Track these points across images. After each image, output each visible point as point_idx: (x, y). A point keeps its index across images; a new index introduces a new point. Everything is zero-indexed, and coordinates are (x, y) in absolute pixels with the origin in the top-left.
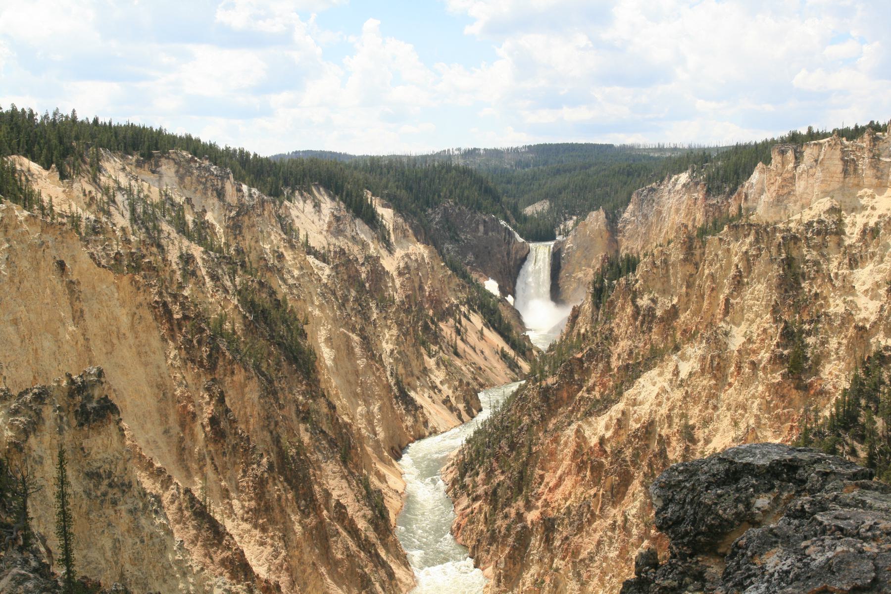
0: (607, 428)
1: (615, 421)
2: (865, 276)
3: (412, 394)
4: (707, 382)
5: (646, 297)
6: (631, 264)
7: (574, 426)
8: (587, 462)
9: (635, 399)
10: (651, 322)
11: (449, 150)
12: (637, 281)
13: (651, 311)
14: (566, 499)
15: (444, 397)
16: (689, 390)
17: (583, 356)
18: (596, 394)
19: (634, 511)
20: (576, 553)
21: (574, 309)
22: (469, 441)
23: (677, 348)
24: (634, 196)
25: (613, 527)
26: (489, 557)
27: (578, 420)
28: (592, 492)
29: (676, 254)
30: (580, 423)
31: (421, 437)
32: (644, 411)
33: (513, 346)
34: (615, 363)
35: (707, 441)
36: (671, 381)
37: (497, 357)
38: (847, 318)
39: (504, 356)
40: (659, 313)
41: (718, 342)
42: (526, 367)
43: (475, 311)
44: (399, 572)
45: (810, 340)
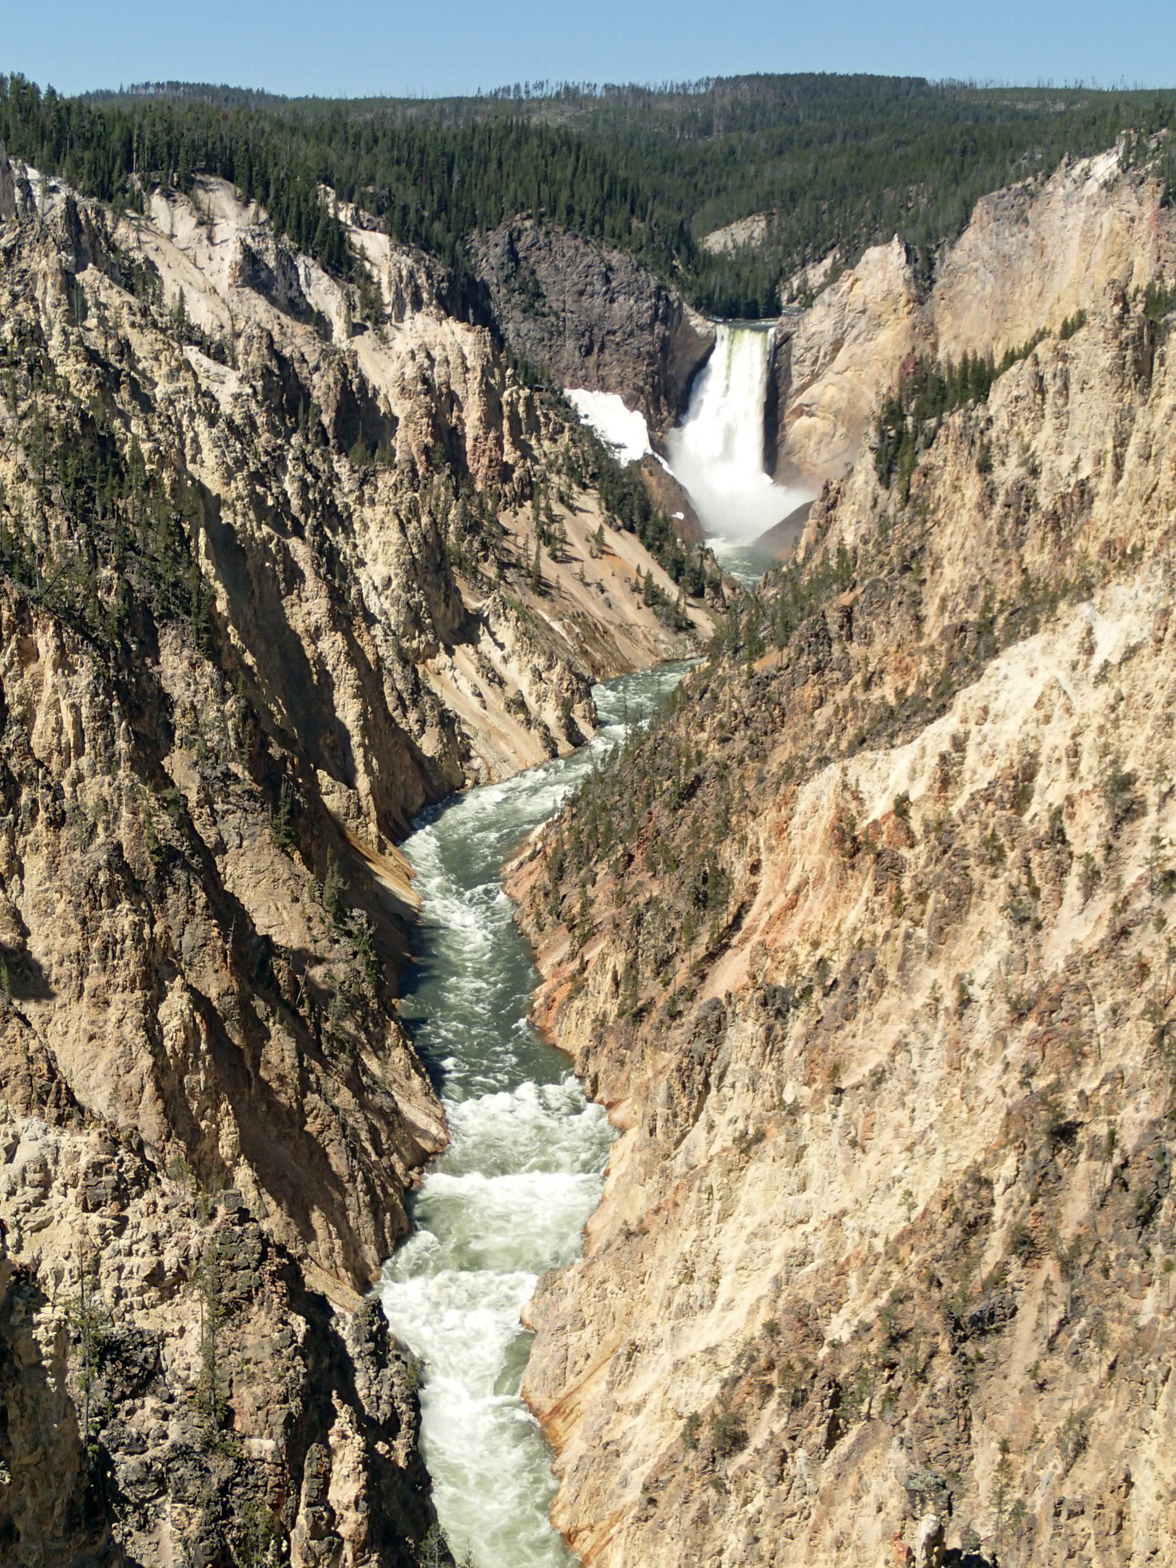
0: (913, 775)
1: (932, 761)
3: (434, 685)
5: (1013, 461)
6: (978, 379)
7: (833, 771)
9: (985, 710)
10: (1020, 521)
11: (517, 87)
12: (990, 421)
13: (1022, 500)
14: (816, 945)
15: (510, 693)
16: (1125, 692)
17: (856, 599)
18: (886, 692)
19: (981, 976)
21: (826, 488)
22: (573, 802)
24: (978, 211)
26: (623, 1078)
27: (842, 756)
28: (881, 930)
29: (1094, 353)
30: (846, 762)
32: (1007, 734)
33: (677, 570)
36: (1074, 668)
37: (639, 598)
39: (653, 598)
40: (1045, 501)
43: (585, 487)
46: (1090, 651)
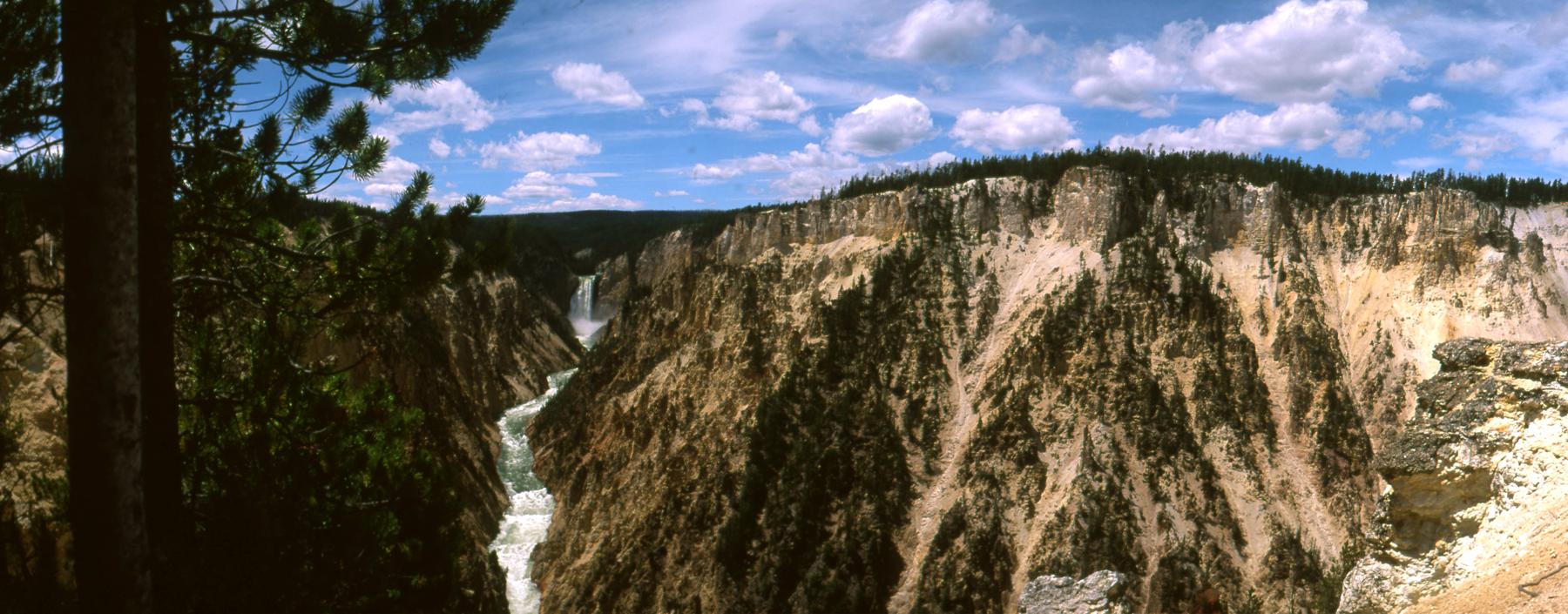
2: (797, 299)
4: (700, 368)
6: (647, 291)
8: (622, 422)
20: (617, 484)
23: (678, 347)
25: (642, 466)
29: (678, 284)
31: (511, 406)
34: (639, 358)
35: (702, 407)
38: (788, 326)
41: (706, 342)
42: (576, 359)
44: (500, 497)
45: (766, 340)
46: (679, 363)
